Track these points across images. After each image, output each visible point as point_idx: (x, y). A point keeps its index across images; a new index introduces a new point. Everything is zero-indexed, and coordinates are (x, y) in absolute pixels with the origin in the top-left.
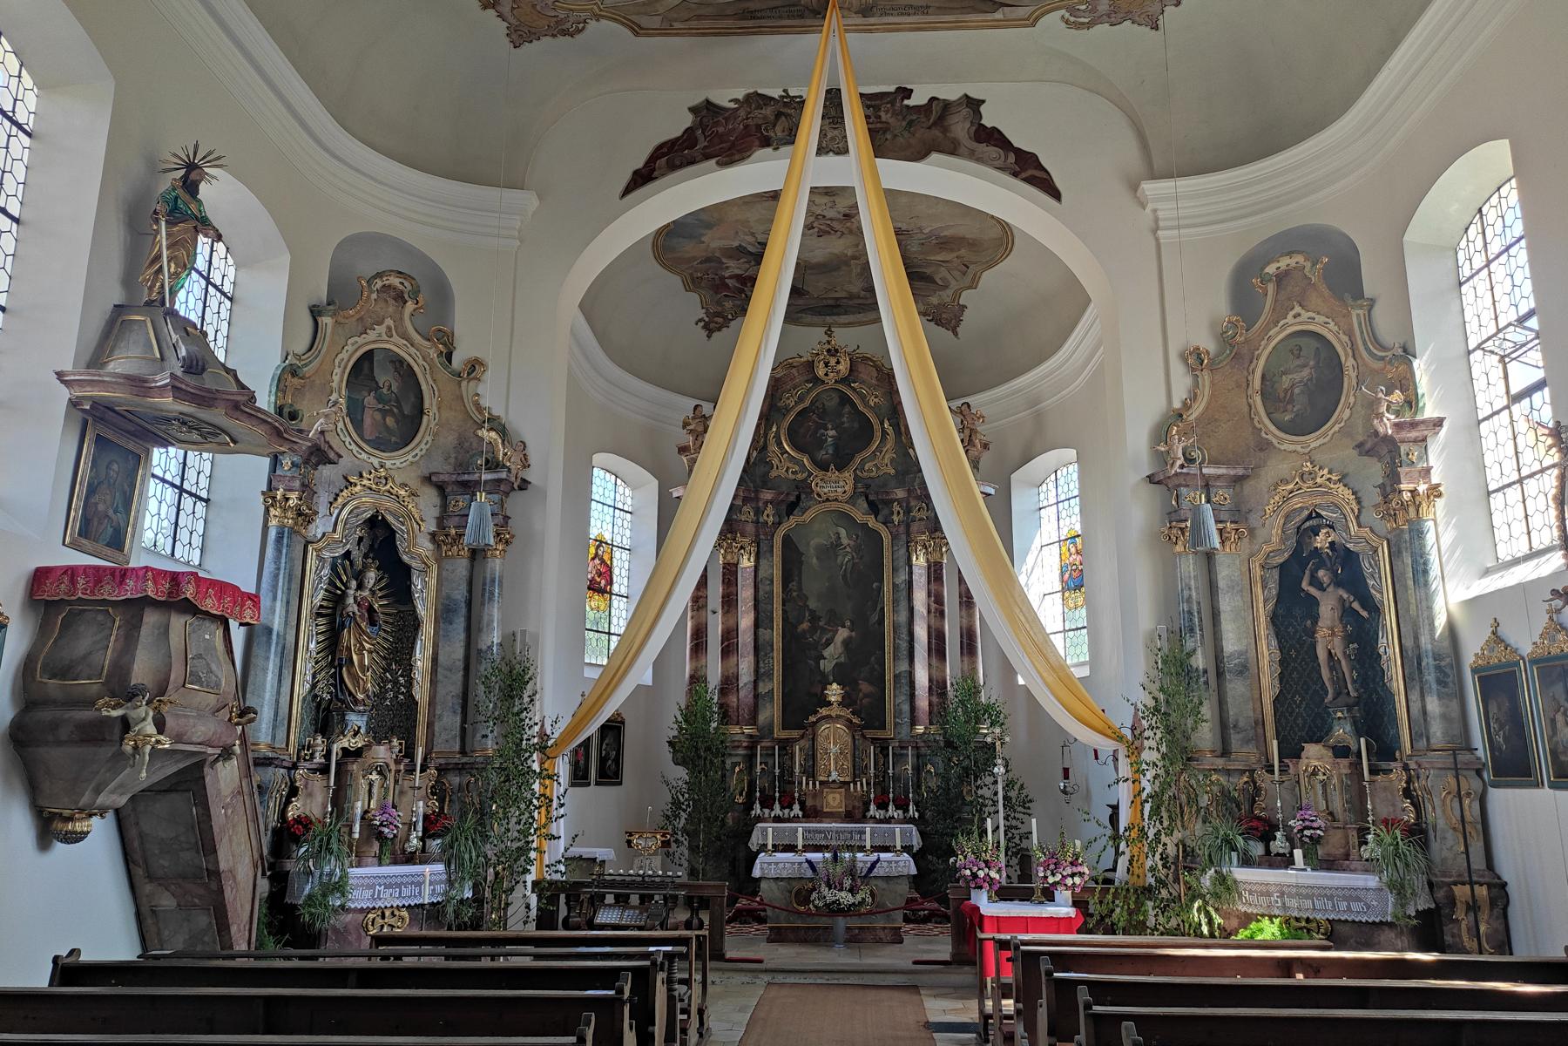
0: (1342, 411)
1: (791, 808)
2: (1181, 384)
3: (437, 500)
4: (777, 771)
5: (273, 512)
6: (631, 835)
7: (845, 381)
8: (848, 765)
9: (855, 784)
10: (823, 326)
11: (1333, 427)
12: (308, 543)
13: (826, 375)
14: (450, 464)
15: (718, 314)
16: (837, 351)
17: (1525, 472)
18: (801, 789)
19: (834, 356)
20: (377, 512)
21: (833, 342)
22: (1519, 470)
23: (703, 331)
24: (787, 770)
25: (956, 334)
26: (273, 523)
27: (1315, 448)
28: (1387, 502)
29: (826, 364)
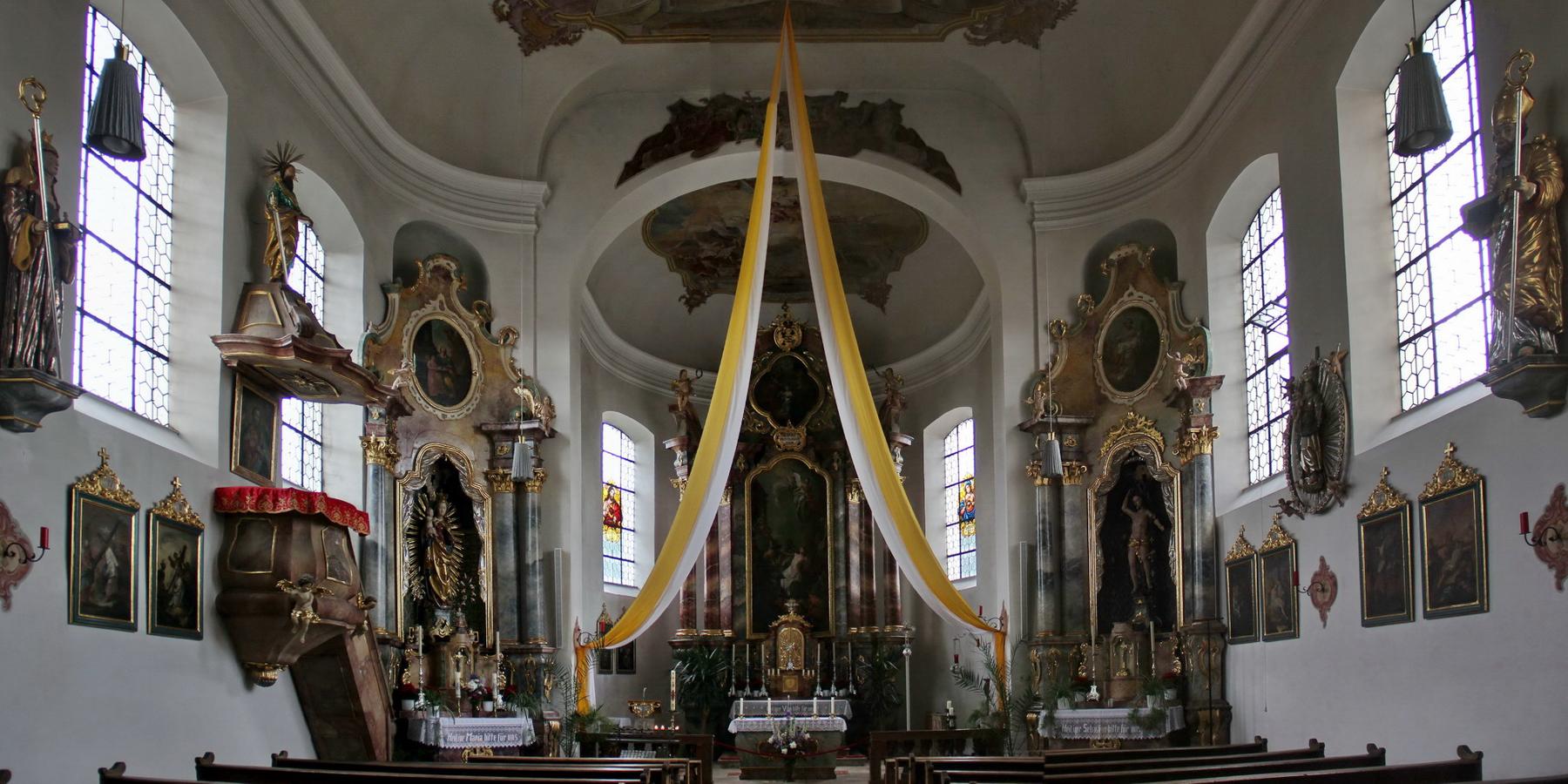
0: (1158, 372)
1: (759, 689)
2: (1046, 350)
3: (487, 446)
4: (748, 662)
5: (369, 454)
6: (632, 703)
7: (798, 349)
8: (801, 658)
9: (806, 671)
10: (779, 302)
11: (1149, 385)
12: (396, 479)
13: (784, 344)
14: (494, 416)
15: (698, 292)
16: (791, 323)
17: (1272, 418)
18: (766, 676)
19: (790, 327)
20: (444, 455)
21: (788, 316)
22: (1268, 416)
23: (684, 307)
24: (755, 662)
25: (883, 310)
26: (370, 461)
27: (1138, 402)
28: (1182, 441)
29: (784, 335)
